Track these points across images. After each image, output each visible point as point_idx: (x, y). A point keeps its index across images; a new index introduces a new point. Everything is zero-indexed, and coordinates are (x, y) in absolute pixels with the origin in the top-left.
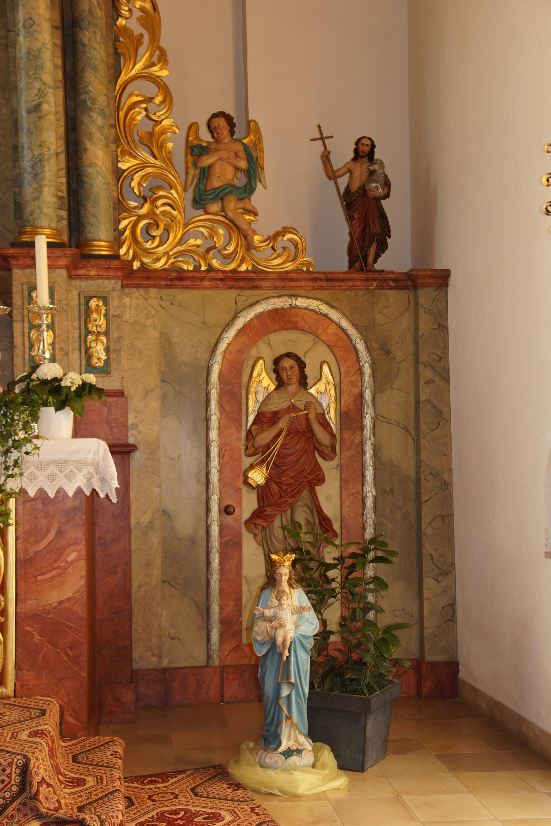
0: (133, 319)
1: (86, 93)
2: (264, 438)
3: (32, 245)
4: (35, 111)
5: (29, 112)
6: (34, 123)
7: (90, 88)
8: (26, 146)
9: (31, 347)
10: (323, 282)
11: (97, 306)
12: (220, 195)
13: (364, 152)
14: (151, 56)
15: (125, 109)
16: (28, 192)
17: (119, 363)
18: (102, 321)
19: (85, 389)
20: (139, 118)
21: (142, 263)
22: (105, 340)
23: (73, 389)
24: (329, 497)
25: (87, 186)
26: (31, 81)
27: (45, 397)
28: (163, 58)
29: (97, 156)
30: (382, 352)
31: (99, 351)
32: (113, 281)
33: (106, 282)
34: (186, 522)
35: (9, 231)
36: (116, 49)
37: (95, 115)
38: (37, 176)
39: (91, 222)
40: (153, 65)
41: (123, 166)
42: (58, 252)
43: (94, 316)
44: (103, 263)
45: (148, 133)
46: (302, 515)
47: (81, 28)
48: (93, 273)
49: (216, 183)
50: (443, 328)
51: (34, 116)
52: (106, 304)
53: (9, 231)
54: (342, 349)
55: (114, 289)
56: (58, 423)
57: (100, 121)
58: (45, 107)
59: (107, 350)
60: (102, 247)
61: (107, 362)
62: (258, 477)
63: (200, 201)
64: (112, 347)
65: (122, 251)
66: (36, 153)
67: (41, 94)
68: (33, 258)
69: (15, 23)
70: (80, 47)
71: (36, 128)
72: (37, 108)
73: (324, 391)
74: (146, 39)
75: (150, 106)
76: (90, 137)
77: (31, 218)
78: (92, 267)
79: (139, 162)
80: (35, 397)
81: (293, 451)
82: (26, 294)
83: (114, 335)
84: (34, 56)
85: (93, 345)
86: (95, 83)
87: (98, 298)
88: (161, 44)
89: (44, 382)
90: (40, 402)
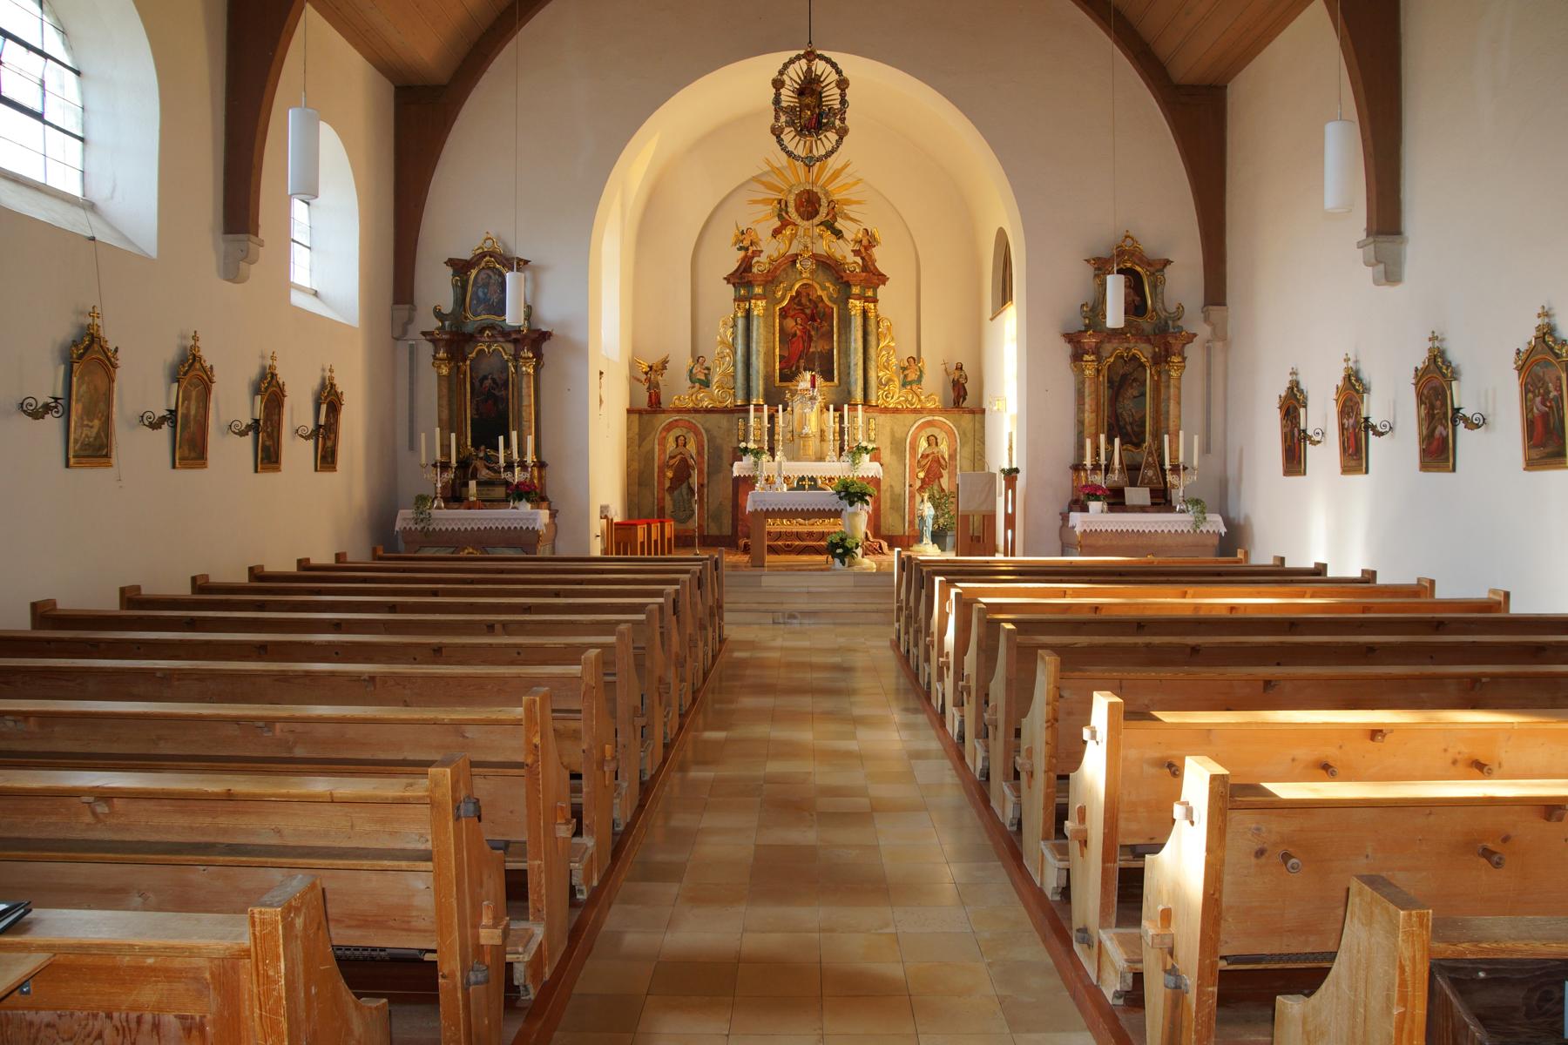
10: (944, 411)
12: (911, 383)
13: (960, 368)
24: (945, 482)
30: (963, 434)
34: (897, 490)
50: (983, 427)
54: (950, 434)
56: (866, 457)
62: (922, 475)
63: (904, 385)
73: (944, 448)
81: (933, 468)
86: (872, 352)
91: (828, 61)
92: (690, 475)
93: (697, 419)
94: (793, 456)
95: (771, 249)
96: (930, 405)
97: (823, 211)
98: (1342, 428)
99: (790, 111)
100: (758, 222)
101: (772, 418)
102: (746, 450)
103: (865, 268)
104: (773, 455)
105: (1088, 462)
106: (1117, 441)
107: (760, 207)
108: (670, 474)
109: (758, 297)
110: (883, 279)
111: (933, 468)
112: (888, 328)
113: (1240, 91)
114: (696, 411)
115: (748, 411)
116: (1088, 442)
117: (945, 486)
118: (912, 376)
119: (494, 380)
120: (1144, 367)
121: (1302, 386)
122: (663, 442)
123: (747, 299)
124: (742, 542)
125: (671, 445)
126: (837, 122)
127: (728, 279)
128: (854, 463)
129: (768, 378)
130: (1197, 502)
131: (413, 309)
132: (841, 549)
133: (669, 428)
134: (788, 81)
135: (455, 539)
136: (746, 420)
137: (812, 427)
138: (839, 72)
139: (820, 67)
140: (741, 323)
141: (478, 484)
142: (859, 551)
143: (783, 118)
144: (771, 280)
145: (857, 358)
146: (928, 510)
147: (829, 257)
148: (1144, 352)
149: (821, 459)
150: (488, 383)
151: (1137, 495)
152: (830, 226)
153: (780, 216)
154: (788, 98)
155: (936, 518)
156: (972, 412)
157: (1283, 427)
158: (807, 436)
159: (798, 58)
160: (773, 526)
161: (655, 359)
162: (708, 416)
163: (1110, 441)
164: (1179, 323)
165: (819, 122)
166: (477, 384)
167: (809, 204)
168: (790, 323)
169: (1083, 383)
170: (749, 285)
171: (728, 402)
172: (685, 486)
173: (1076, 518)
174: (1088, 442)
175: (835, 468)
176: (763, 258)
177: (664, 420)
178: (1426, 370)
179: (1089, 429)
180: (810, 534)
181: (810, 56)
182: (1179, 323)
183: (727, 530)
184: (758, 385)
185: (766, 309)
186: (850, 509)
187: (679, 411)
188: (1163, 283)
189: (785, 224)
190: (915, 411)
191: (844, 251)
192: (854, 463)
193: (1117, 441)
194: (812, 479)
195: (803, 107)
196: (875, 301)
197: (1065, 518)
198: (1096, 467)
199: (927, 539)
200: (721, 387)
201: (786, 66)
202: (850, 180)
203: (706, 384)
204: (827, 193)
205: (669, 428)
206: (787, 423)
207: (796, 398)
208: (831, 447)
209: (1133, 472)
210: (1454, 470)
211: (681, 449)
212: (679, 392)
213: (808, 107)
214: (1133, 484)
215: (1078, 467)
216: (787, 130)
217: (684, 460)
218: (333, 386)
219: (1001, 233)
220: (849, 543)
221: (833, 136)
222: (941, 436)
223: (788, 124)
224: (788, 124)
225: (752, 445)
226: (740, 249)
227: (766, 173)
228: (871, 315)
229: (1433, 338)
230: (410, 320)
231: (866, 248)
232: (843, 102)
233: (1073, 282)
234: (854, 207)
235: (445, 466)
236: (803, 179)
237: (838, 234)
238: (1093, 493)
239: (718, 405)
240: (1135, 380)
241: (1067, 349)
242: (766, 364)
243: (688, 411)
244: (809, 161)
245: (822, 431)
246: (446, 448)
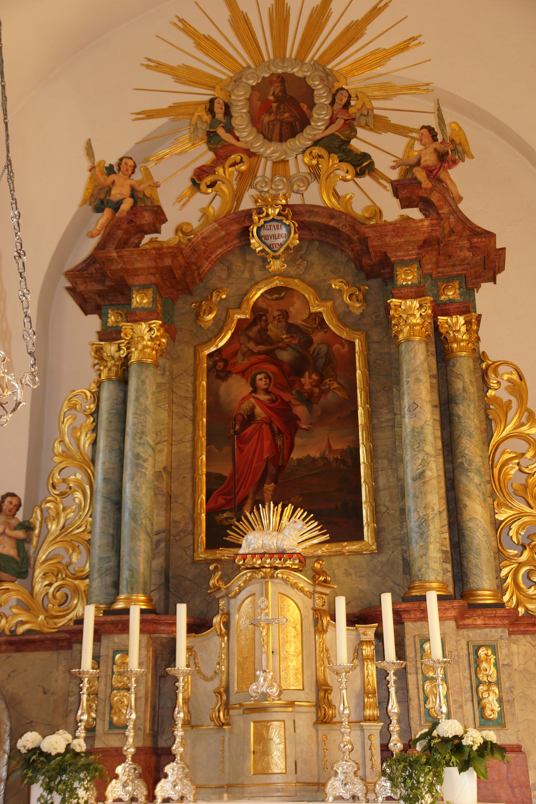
0: (522, 667)
1: (463, 456)
3: (423, 599)
4: (420, 478)
5: (414, 480)
6: (419, 488)
7: (466, 452)
8: (412, 509)
9: (426, 699)
11: (486, 655)
14: (520, 418)
15: (499, 466)
16: (416, 549)
17: (513, 715)
18: (492, 670)
19: (487, 747)
20: (512, 472)
21: (527, 610)
22: (497, 691)
23: (475, 748)
25: (468, 539)
26: (415, 453)
27: (447, 756)
28: (532, 418)
29: (476, 511)
31: (491, 701)
32: (500, 630)
33: (493, 630)
35: (398, 585)
36: (487, 416)
37: (472, 475)
38: (423, 535)
39: (474, 572)
40: (523, 425)
41: (500, 517)
42: (447, 604)
43: (484, 665)
44: (490, 612)
45: (521, 485)
47: (456, 404)
48: (479, 622)
51: (418, 483)
52: (495, 653)
53: (398, 585)
55: (501, 638)
57: (477, 480)
58: (428, 473)
59: (500, 700)
60: (486, 597)
61: (501, 713)
64: (504, 697)
65: (506, 598)
66: (421, 515)
67: (424, 463)
68: (424, 611)
69: (401, 409)
70: (456, 419)
71: (421, 493)
72: (421, 475)
74: (515, 404)
75: (523, 461)
76: (469, 494)
77: (419, 573)
78: (479, 616)
79: (515, 512)
80: (437, 756)
82: (418, 646)
83: (506, 685)
84: (417, 433)
85: (485, 695)
86: (471, 448)
87: (487, 646)
88: (529, 406)
89: (445, 740)
90: (444, 762)
109: (135, 317)
152: (338, 146)
153: (211, 137)
158: (258, 708)
168: (236, 390)
189: (222, 152)
196: (467, 308)
204: (328, 77)
237: (362, 165)
245: (323, 689)
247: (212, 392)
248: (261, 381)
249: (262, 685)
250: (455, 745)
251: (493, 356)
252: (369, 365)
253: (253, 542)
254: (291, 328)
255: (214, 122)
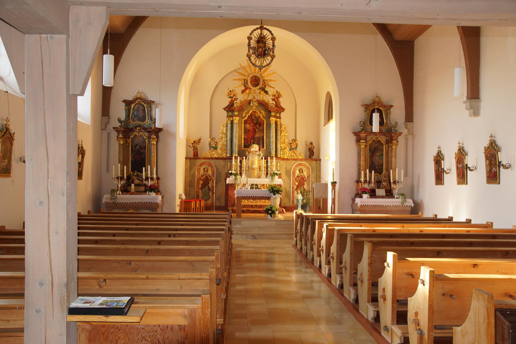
2: (298, 179)
10: (305, 160)
12: (293, 149)
13: (311, 143)
16: (271, 151)
24: (305, 187)
28: (286, 132)
29: (279, 146)
30: (313, 168)
31: (279, 169)
34: (288, 189)
46: (302, 188)
49: (292, 147)
50: (320, 166)
54: (307, 168)
56: (277, 177)
62: (297, 184)
63: (290, 150)
73: (305, 173)
81: (301, 181)
86: (279, 137)
91: (268, 30)
92: (209, 183)
93: (212, 162)
94: (249, 176)
95: (241, 98)
96: (300, 157)
97: (261, 84)
98: (457, 168)
99: (254, 48)
100: (236, 87)
101: (241, 162)
102: (231, 174)
103: (276, 106)
104: (241, 176)
105: (362, 179)
106: (373, 172)
107: (237, 82)
108: (201, 182)
109: (236, 116)
110: (283, 110)
111: (301, 181)
112: (285, 128)
113: (420, 43)
114: (211, 158)
115: (232, 159)
116: (362, 172)
117: (306, 188)
118: (293, 147)
119: (140, 146)
120: (383, 145)
121: (442, 152)
122: (199, 170)
123: (232, 116)
124: (230, 208)
125: (202, 172)
126: (271, 53)
127: (225, 109)
128: (272, 179)
129: (240, 146)
130: (403, 195)
131: (109, 118)
132: (270, 211)
133: (201, 165)
134: (253, 37)
135: (126, 206)
136: (231, 163)
137: (256, 166)
138: (272, 34)
139: (265, 32)
140: (229, 126)
141: (135, 185)
142: (277, 212)
143: (251, 51)
144: (241, 109)
145: (273, 140)
146: (300, 197)
147: (263, 101)
148: (383, 139)
149: (259, 177)
150: (138, 147)
151: (380, 192)
153: (244, 85)
154: (253, 43)
155: (303, 200)
156: (316, 160)
157: (435, 167)
158: (254, 169)
159: (257, 29)
160: (245, 202)
161: (196, 139)
162: (216, 160)
163: (370, 172)
164: (396, 128)
165: (265, 53)
166: (134, 147)
167: (256, 81)
168: (248, 126)
169: (360, 150)
170: (233, 111)
171: (224, 155)
172: (207, 187)
173: (358, 200)
174: (362, 172)
175: (266, 181)
176: (238, 101)
177: (199, 162)
178: (489, 147)
179: (363, 167)
180: (256, 206)
181: (262, 28)
182: (396, 128)
183: (223, 204)
184: (236, 149)
185: (239, 120)
186: (273, 196)
187: (205, 158)
188: (390, 113)
189: (246, 88)
190: (294, 160)
191: (268, 99)
192: (272, 179)
193: (373, 172)
194: (256, 185)
195: (259, 47)
196: (280, 118)
197: (353, 200)
198: (365, 181)
199: (300, 208)
200: (221, 149)
201: (252, 32)
202: (271, 72)
203: (216, 148)
204: (262, 77)
205: (201, 165)
206: (247, 164)
207: (250, 154)
208: (263, 173)
209: (379, 183)
210: (499, 183)
211: (206, 173)
212: (205, 151)
213: (261, 47)
214: (379, 188)
215: (358, 181)
216: (253, 55)
217: (207, 177)
218: (82, 147)
219: (328, 94)
220: (274, 209)
221: (269, 58)
222: (304, 169)
223: (253, 53)
224: (253, 53)
225: (234, 172)
226: (230, 97)
227: (239, 69)
228: (279, 123)
229: (491, 136)
230: (108, 122)
231: (277, 98)
232: (274, 45)
233: (358, 114)
234: (272, 82)
235: (122, 178)
236: (253, 72)
237: (266, 92)
238: (364, 191)
239: (220, 156)
240: (379, 149)
241: (354, 138)
242: (239, 141)
243: (209, 159)
244: (261, 67)
245: (260, 167)
246: (122, 171)
247: (244, 126)
248: (251, 125)
249: (254, 166)
250: (277, 174)
251: (282, 123)
252: (266, 124)
253: (252, 150)
254: (256, 117)
255: (245, 83)
